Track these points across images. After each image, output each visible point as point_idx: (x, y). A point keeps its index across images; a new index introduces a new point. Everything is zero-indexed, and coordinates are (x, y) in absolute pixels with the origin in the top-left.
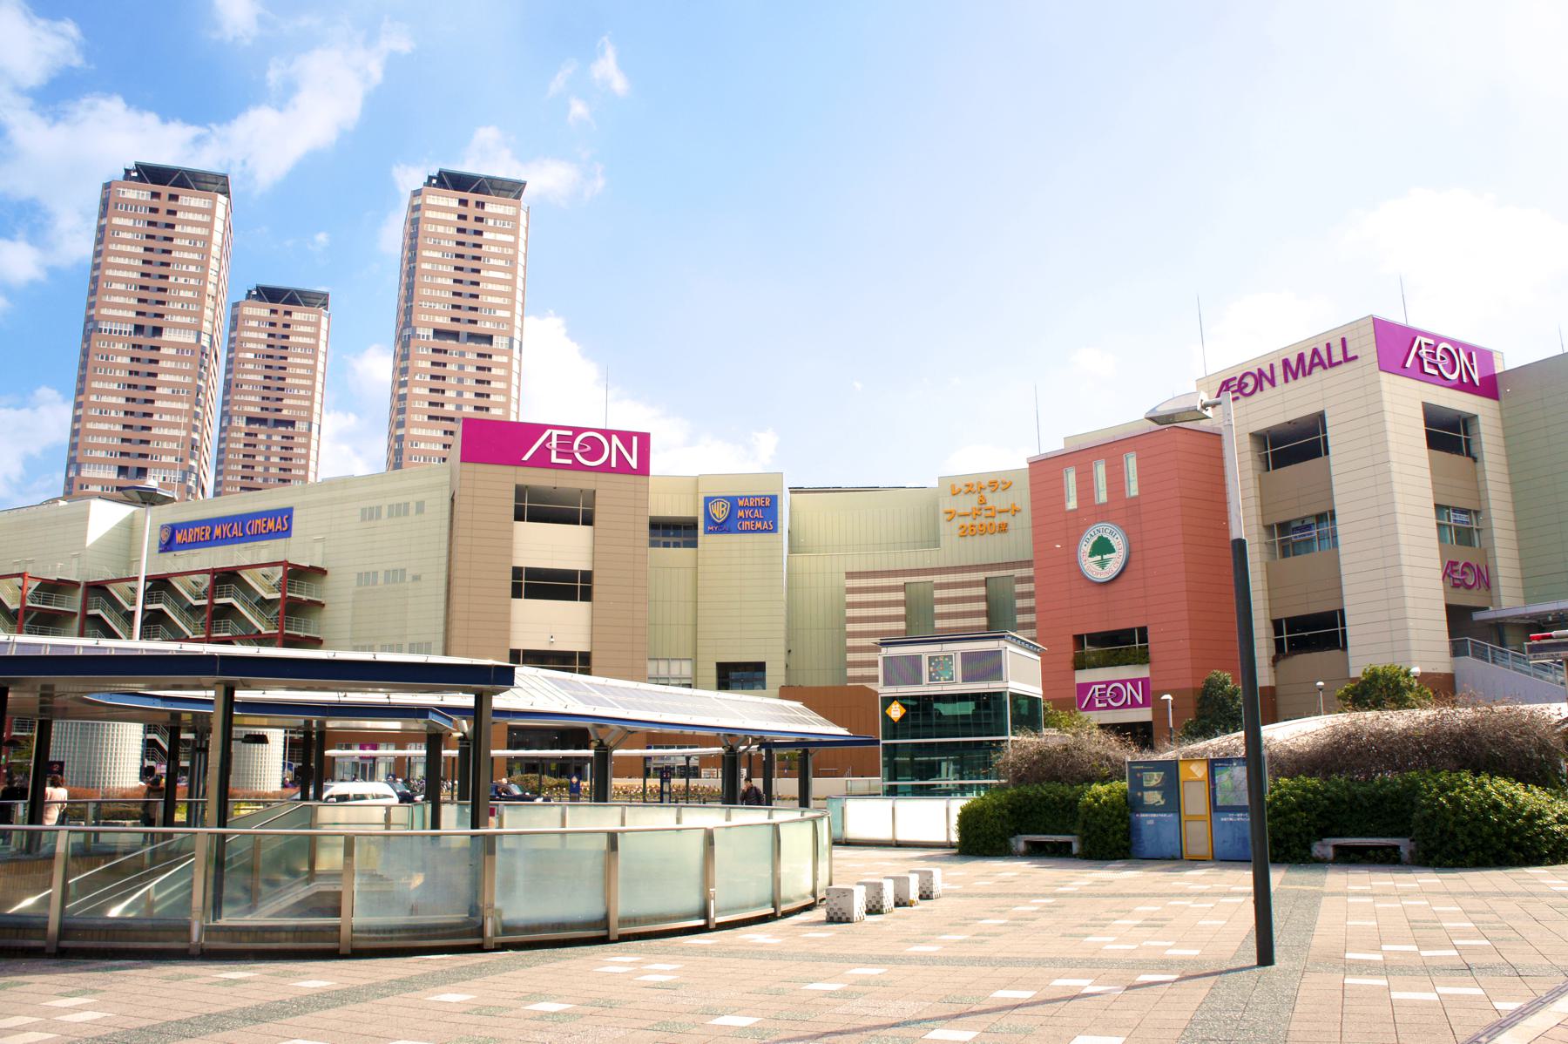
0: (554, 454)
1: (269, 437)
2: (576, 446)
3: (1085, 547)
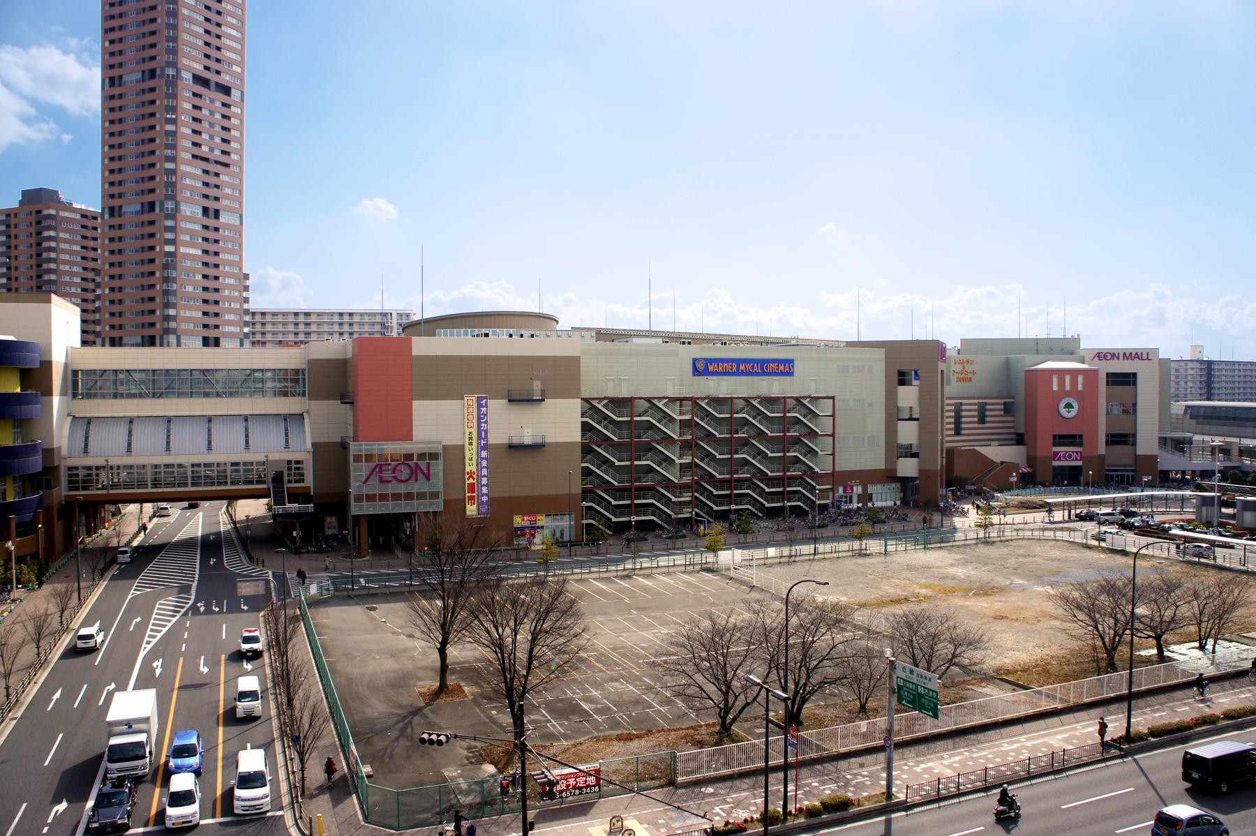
3: (1062, 405)
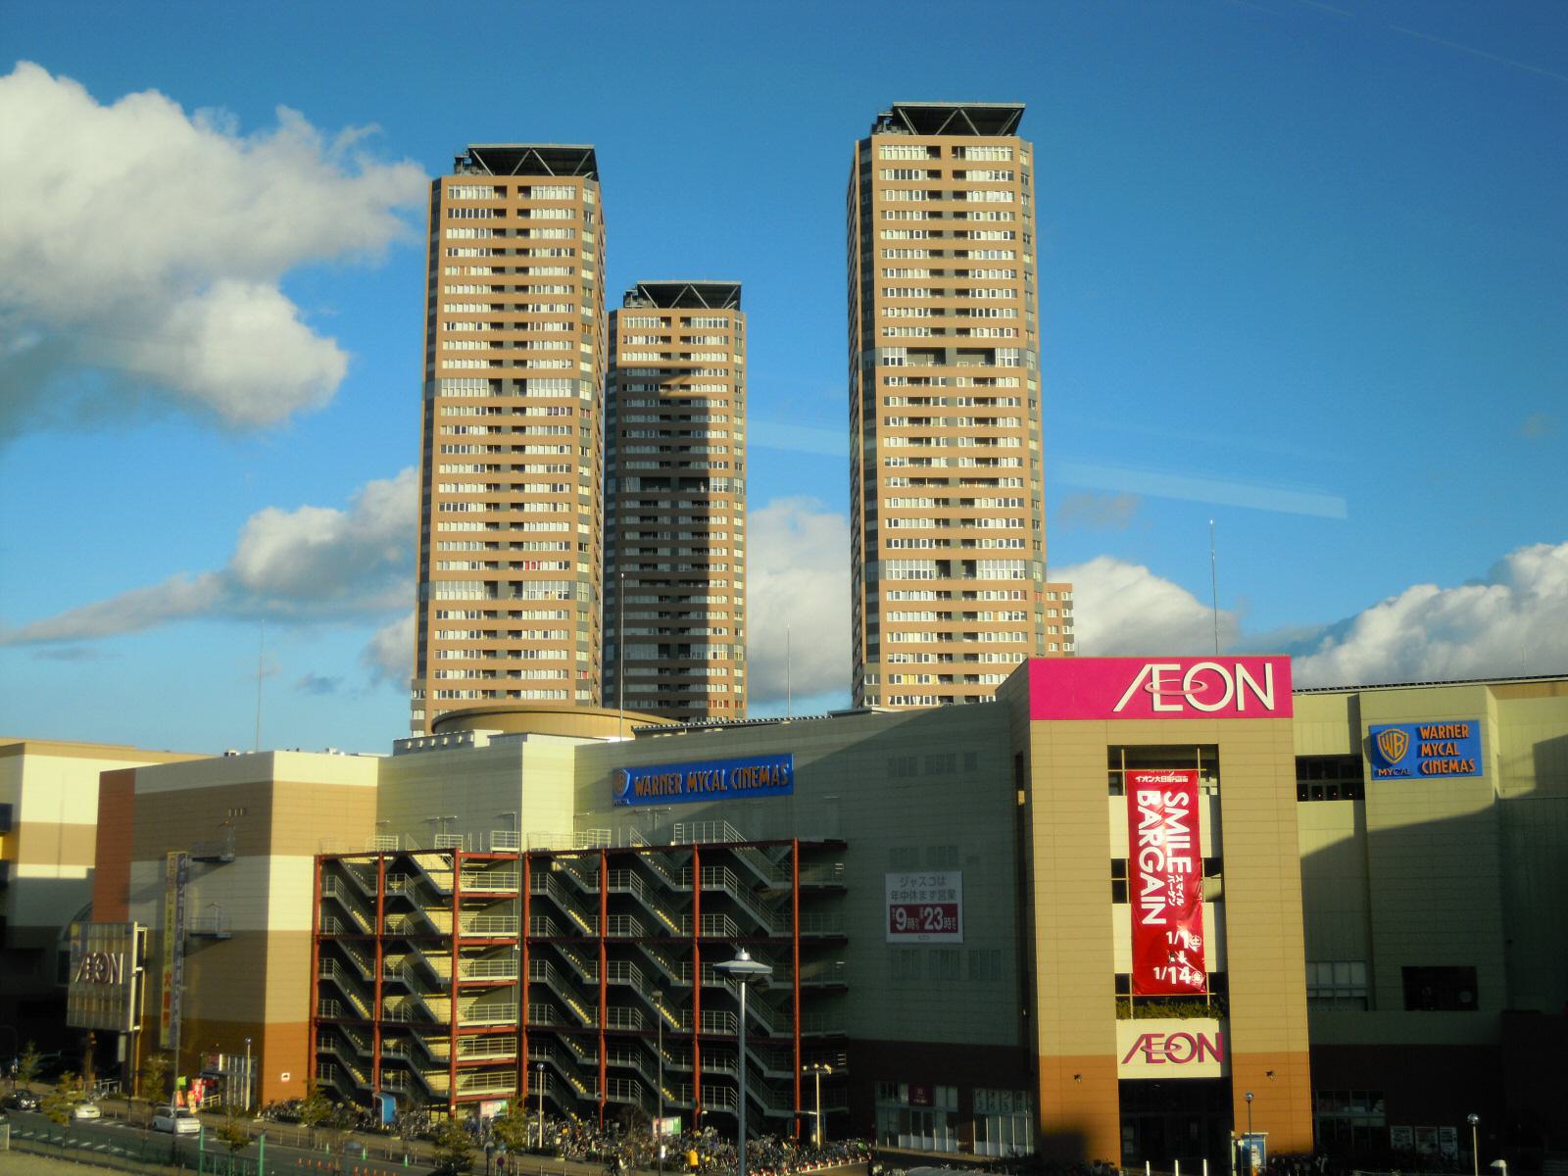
0: (1157, 698)
1: (674, 504)
2: (1187, 686)
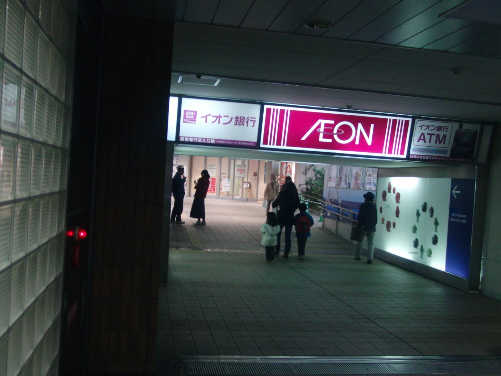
0: (321, 135)
2: (335, 131)
